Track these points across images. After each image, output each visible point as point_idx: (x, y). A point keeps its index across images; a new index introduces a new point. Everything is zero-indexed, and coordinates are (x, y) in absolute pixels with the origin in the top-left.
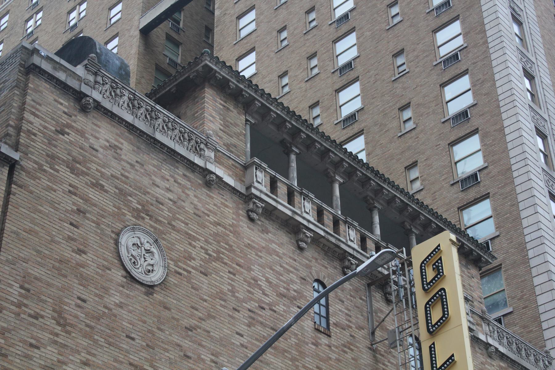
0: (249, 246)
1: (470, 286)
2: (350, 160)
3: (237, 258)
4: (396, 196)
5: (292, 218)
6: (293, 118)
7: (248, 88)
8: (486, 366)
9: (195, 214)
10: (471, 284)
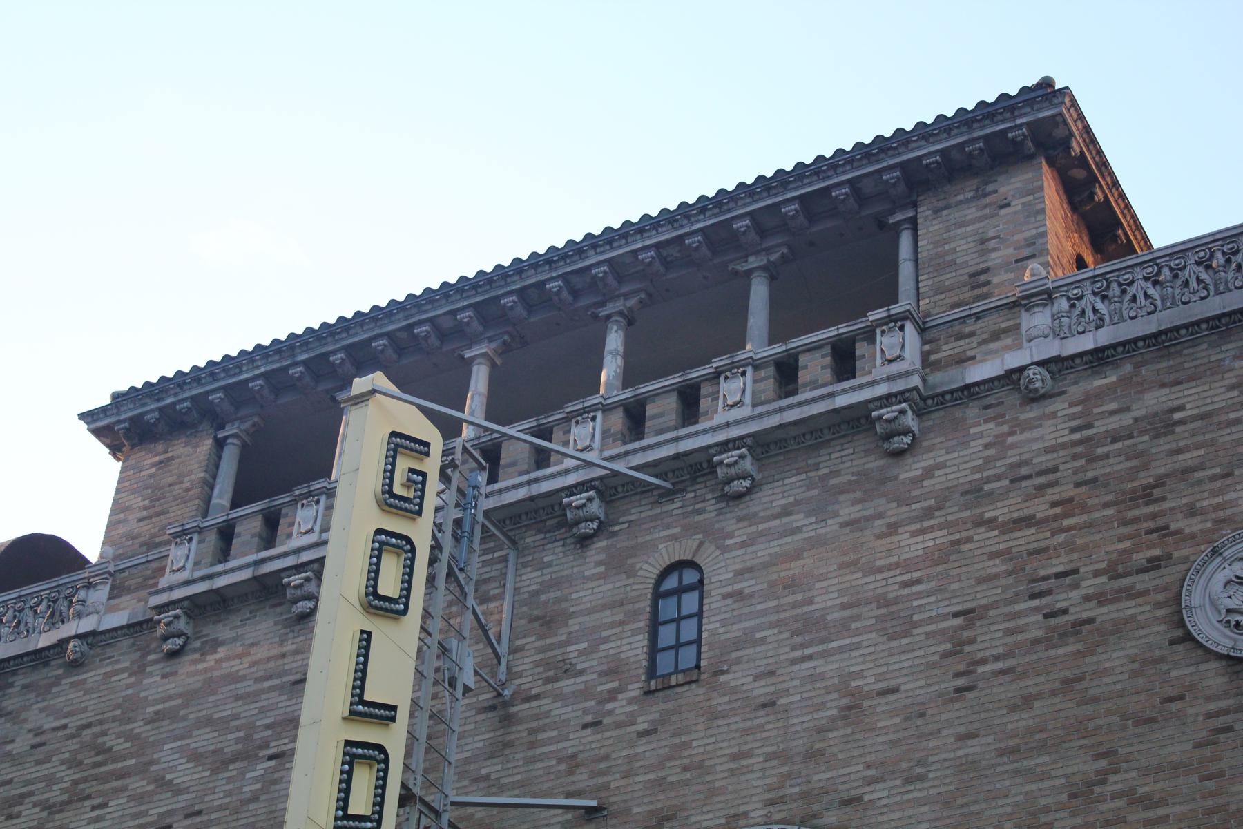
0: (158, 717)
1: (983, 241)
2: (469, 297)
3: (120, 765)
4: (635, 252)
5: (254, 578)
6: (298, 350)
7: (183, 390)
8: (1010, 440)
9: (34, 747)
10: (991, 234)
